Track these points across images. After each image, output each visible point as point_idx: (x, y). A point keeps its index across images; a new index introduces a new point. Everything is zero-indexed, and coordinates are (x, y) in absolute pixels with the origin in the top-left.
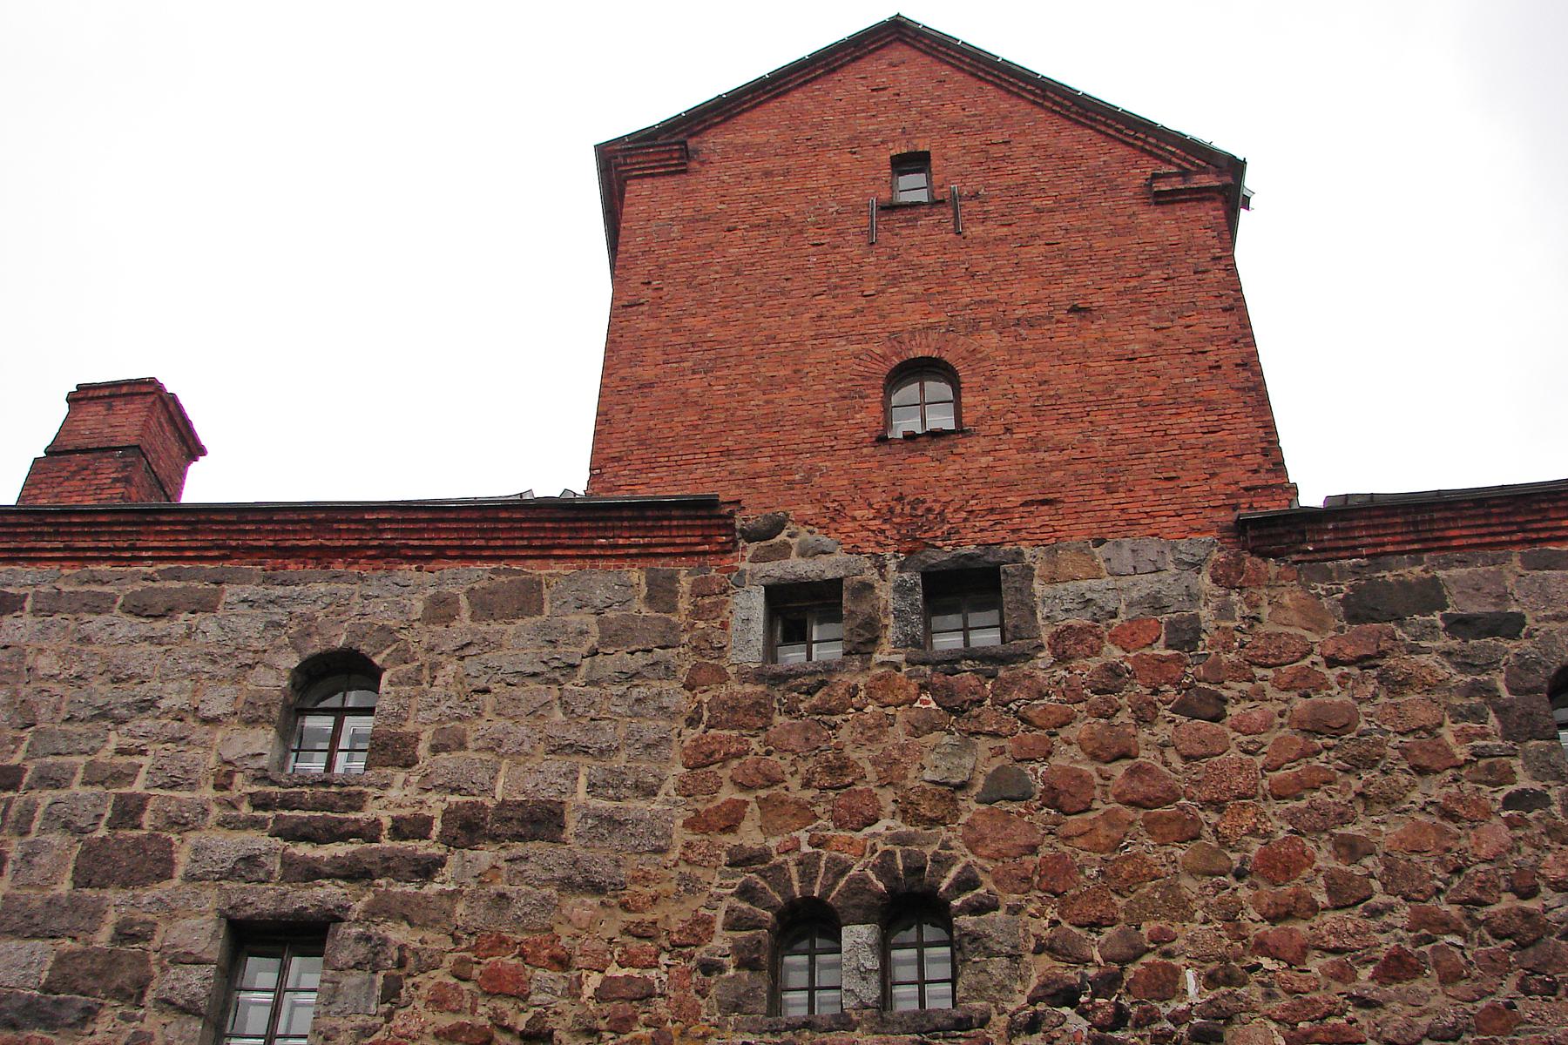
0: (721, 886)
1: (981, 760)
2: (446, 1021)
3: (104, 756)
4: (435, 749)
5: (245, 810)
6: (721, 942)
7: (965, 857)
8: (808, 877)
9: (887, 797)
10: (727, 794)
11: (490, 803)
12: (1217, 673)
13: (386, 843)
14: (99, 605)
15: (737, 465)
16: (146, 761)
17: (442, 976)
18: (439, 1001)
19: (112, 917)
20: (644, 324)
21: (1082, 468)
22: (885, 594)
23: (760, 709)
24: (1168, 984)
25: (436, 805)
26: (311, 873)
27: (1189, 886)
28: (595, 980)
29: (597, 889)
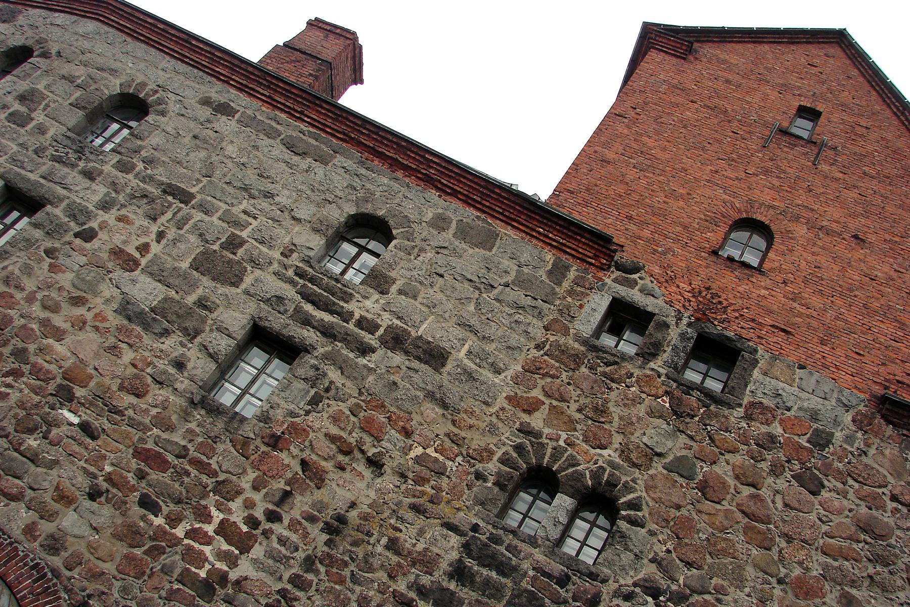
1: (677, 447)
2: (334, 430)
3: (235, 210)
4: (400, 292)
5: (290, 273)
6: (492, 467)
7: (640, 492)
8: (555, 457)
9: (617, 439)
10: (537, 393)
11: (414, 334)
12: (827, 469)
13: (351, 326)
14: (271, 134)
15: (632, 227)
16: (255, 223)
17: (344, 407)
18: (335, 419)
19: (200, 291)
20: (621, 128)
21: (814, 323)
22: (673, 334)
23: (577, 360)
25: (386, 320)
26: (307, 321)
28: (419, 451)
29: (445, 406)
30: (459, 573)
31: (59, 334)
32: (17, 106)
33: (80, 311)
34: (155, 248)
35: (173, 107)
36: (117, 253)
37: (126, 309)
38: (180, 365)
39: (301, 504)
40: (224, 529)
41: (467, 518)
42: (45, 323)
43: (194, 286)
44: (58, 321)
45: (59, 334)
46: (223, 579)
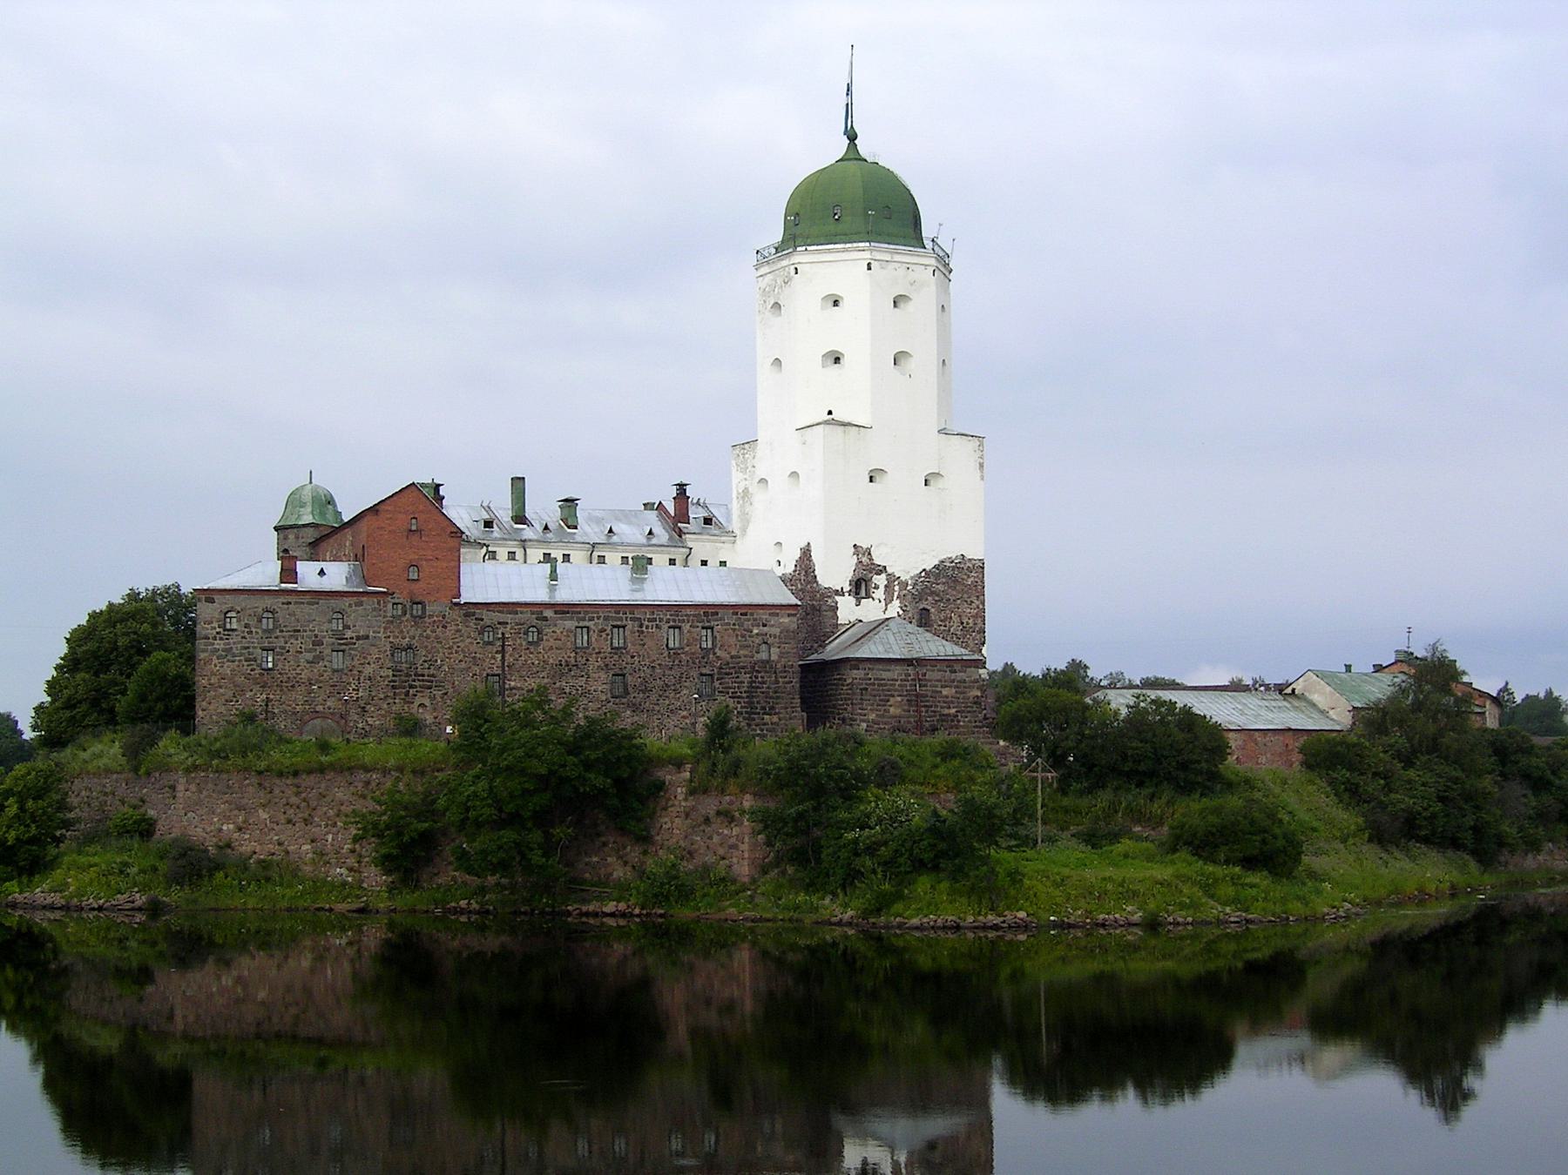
0: (388, 646)
6: (388, 653)
7: (416, 644)
10: (389, 634)
12: (447, 622)
14: (303, 603)
23: (392, 622)
24: (436, 661)
27: (441, 650)
30: (394, 675)
31: (301, 674)
32: (246, 630)
33: (300, 668)
34: (303, 646)
35: (278, 610)
36: (297, 652)
38: (325, 666)
39: (362, 679)
40: (353, 690)
41: (390, 665)
42: (297, 674)
43: (316, 650)
44: (297, 672)
46: (358, 698)
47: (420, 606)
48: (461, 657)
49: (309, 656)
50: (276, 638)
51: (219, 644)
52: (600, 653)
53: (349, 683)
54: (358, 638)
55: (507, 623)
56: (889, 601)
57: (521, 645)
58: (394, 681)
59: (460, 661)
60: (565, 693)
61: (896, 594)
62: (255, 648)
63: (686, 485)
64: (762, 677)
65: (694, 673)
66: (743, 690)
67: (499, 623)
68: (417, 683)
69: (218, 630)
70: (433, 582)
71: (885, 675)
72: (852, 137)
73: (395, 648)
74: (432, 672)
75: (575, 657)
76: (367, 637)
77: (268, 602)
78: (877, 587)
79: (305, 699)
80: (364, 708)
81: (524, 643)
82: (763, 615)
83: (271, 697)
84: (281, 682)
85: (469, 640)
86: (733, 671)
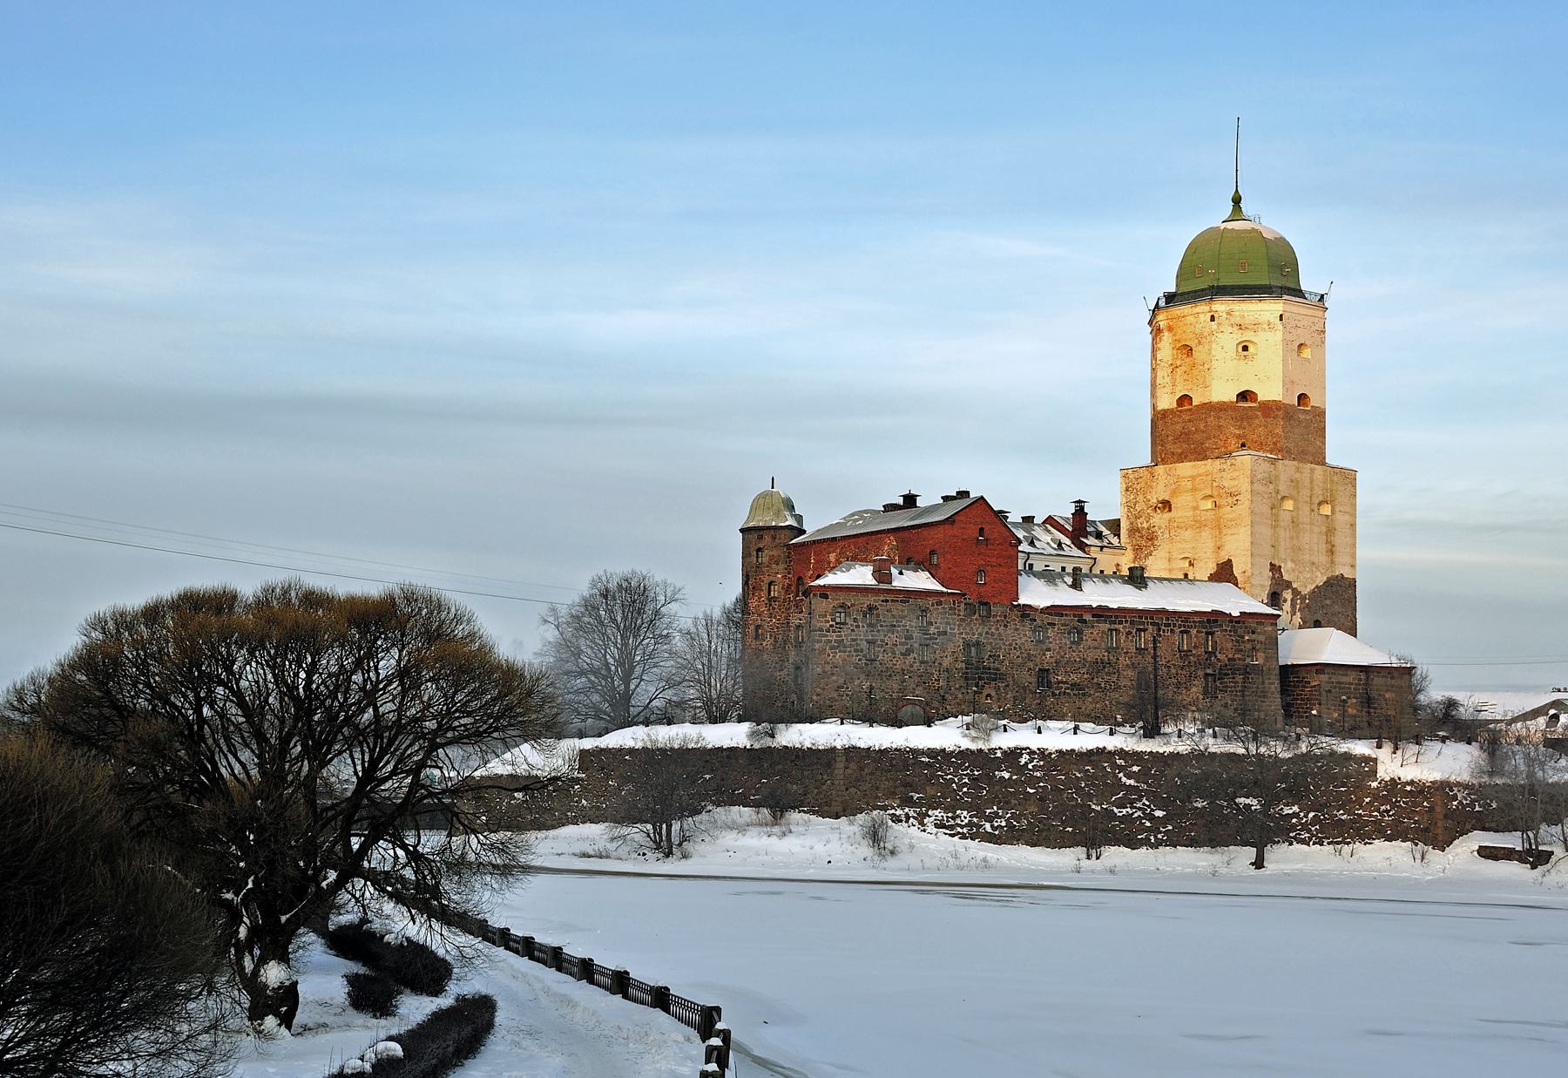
1: (986, 629)
12: (1008, 622)
26: (926, 639)
31: (896, 665)
36: (893, 645)
37: (902, 654)
38: (915, 659)
42: (893, 664)
45: (896, 665)
47: (985, 607)
48: (1018, 654)
49: (903, 649)
50: (878, 631)
51: (833, 637)
52: (1128, 652)
53: (933, 674)
54: (939, 634)
55: (1055, 624)
56: (1294, 613)
57: (1066, 644)
58: (967, 673)
59: (1018, 657)
60: (1101, 688)
61: (1298, 606)
62: (860, 640)
63: (1084, 502)
64: (1252, 678)
65: (1200, 673)
66: (1238, 689)
67: (1049, 624)
68: (985, 676)
69: (831, 623)
70: (996, 585)
71: (1345, 679)
72: (1237, 200)
73: (967, 645)
74: (996, 665)
75: (1108, 656)
76: (945, 633)
77: (871, 600)
78: (1285, 601)
79: (901, 687)
80: (943, 696)
81: (1068, 643)
82: (1252, 623)
83: (874, 684)
84: (882, 671)
85: (1024, 639)
86: (1230, 672)
